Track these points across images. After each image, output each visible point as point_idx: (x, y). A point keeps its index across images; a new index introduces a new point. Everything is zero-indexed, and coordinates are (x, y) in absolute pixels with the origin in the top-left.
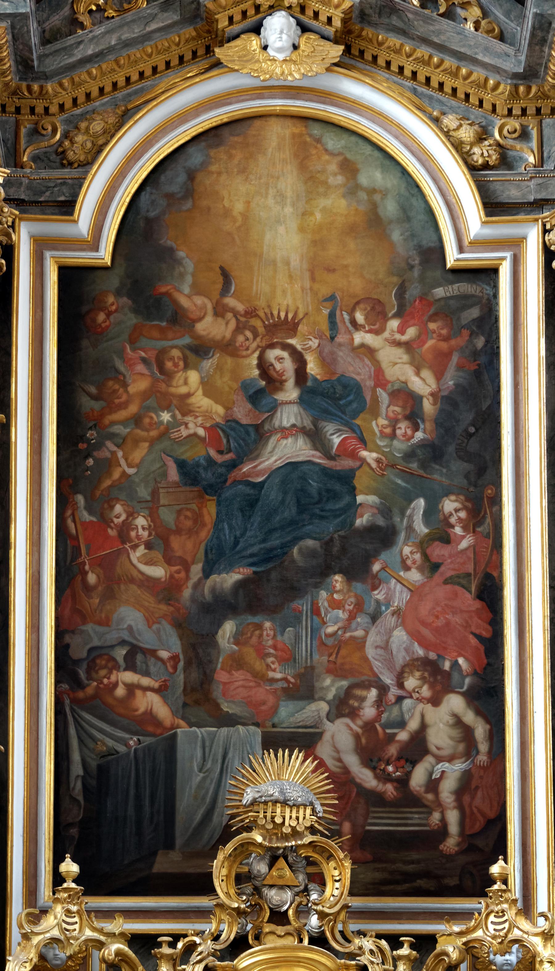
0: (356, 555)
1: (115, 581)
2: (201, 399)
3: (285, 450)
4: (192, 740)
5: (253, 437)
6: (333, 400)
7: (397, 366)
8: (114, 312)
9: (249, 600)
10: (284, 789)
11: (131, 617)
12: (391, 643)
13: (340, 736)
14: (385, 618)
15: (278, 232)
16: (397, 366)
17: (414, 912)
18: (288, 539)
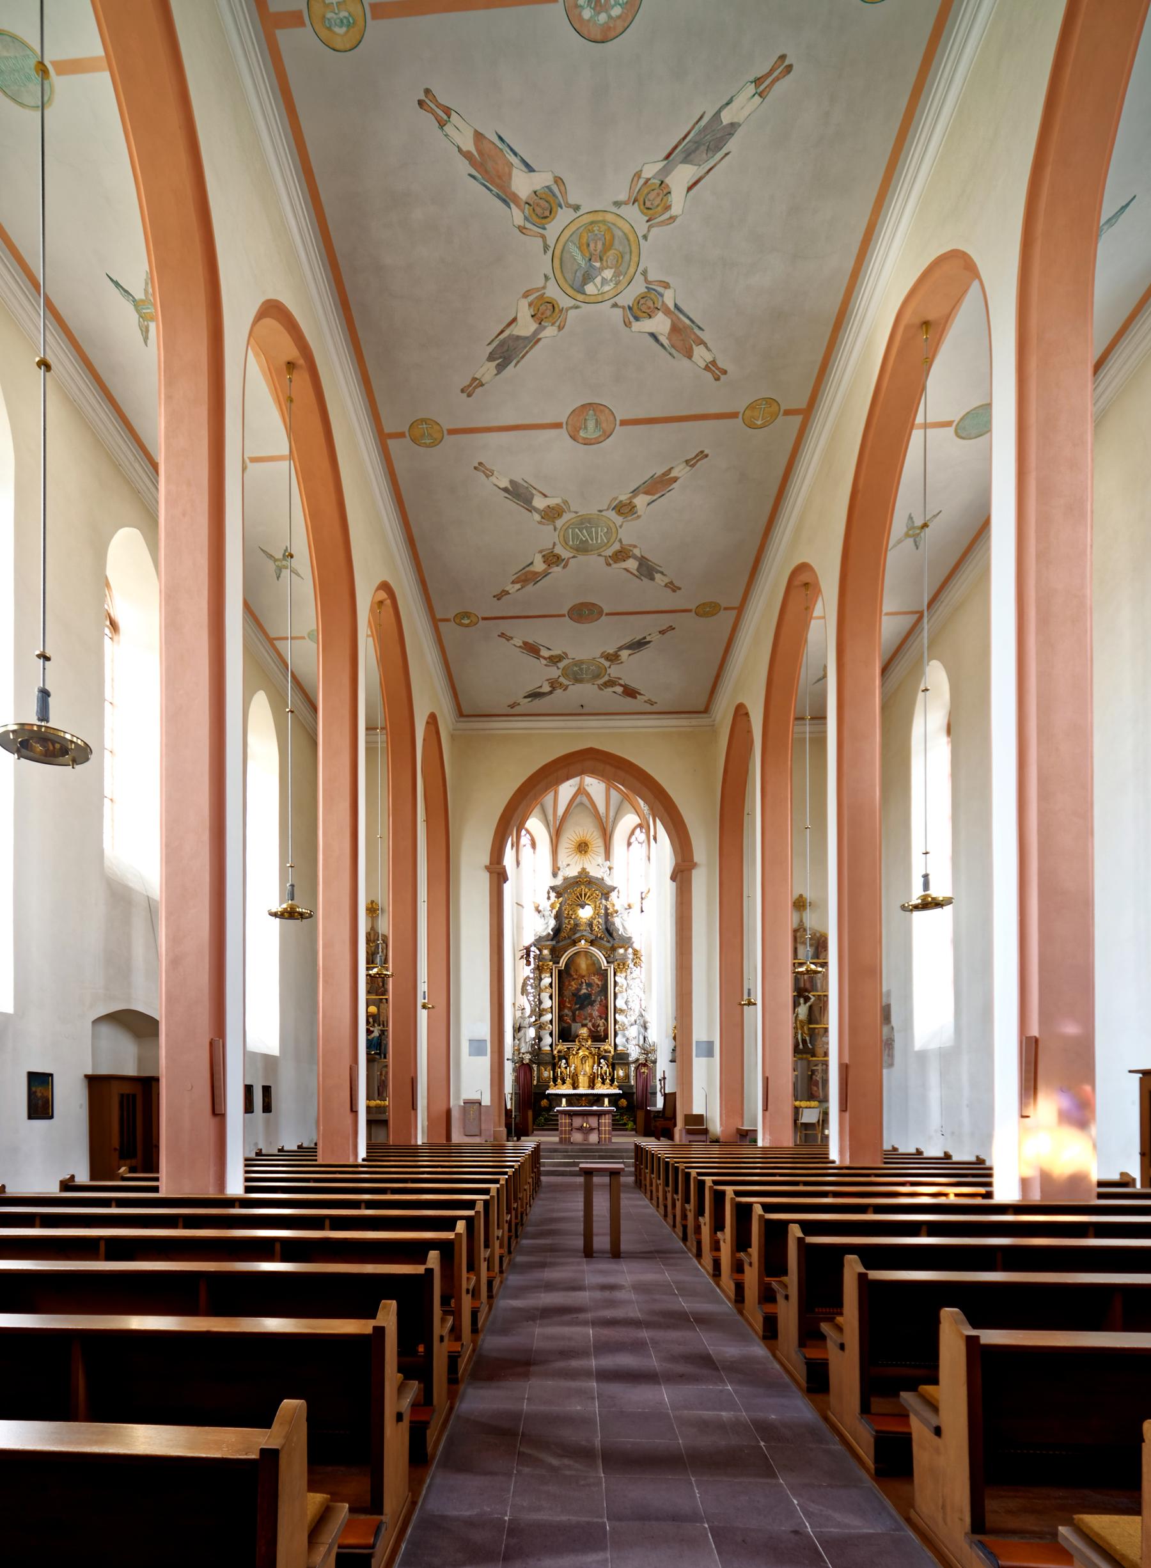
0: (592, 1003)
1: (565, 1007)
2: (574, 985)
3: (584, 991)
4: (574, 1026)
5: (580, 990)
6: (589, 985)
7: (597, 981)
8: (564, 975)
9: (580, 1009)
10: (584, 1032)
11: (566, 1011)
12: (596, 1014)
13: (590, 1025)
14: (595, 1011)
15: (583, 964)
16: (597, 981)
17: (598, 1044)
18: (584, 1001)
